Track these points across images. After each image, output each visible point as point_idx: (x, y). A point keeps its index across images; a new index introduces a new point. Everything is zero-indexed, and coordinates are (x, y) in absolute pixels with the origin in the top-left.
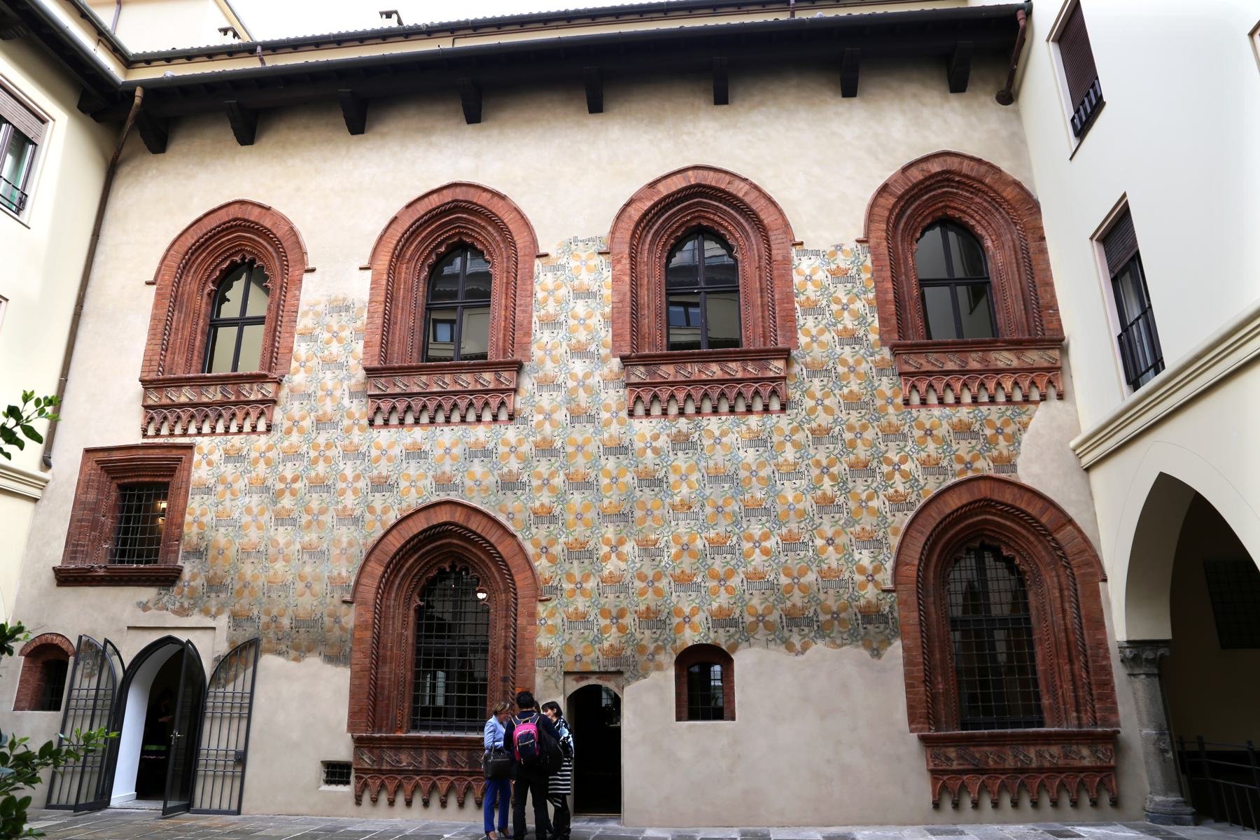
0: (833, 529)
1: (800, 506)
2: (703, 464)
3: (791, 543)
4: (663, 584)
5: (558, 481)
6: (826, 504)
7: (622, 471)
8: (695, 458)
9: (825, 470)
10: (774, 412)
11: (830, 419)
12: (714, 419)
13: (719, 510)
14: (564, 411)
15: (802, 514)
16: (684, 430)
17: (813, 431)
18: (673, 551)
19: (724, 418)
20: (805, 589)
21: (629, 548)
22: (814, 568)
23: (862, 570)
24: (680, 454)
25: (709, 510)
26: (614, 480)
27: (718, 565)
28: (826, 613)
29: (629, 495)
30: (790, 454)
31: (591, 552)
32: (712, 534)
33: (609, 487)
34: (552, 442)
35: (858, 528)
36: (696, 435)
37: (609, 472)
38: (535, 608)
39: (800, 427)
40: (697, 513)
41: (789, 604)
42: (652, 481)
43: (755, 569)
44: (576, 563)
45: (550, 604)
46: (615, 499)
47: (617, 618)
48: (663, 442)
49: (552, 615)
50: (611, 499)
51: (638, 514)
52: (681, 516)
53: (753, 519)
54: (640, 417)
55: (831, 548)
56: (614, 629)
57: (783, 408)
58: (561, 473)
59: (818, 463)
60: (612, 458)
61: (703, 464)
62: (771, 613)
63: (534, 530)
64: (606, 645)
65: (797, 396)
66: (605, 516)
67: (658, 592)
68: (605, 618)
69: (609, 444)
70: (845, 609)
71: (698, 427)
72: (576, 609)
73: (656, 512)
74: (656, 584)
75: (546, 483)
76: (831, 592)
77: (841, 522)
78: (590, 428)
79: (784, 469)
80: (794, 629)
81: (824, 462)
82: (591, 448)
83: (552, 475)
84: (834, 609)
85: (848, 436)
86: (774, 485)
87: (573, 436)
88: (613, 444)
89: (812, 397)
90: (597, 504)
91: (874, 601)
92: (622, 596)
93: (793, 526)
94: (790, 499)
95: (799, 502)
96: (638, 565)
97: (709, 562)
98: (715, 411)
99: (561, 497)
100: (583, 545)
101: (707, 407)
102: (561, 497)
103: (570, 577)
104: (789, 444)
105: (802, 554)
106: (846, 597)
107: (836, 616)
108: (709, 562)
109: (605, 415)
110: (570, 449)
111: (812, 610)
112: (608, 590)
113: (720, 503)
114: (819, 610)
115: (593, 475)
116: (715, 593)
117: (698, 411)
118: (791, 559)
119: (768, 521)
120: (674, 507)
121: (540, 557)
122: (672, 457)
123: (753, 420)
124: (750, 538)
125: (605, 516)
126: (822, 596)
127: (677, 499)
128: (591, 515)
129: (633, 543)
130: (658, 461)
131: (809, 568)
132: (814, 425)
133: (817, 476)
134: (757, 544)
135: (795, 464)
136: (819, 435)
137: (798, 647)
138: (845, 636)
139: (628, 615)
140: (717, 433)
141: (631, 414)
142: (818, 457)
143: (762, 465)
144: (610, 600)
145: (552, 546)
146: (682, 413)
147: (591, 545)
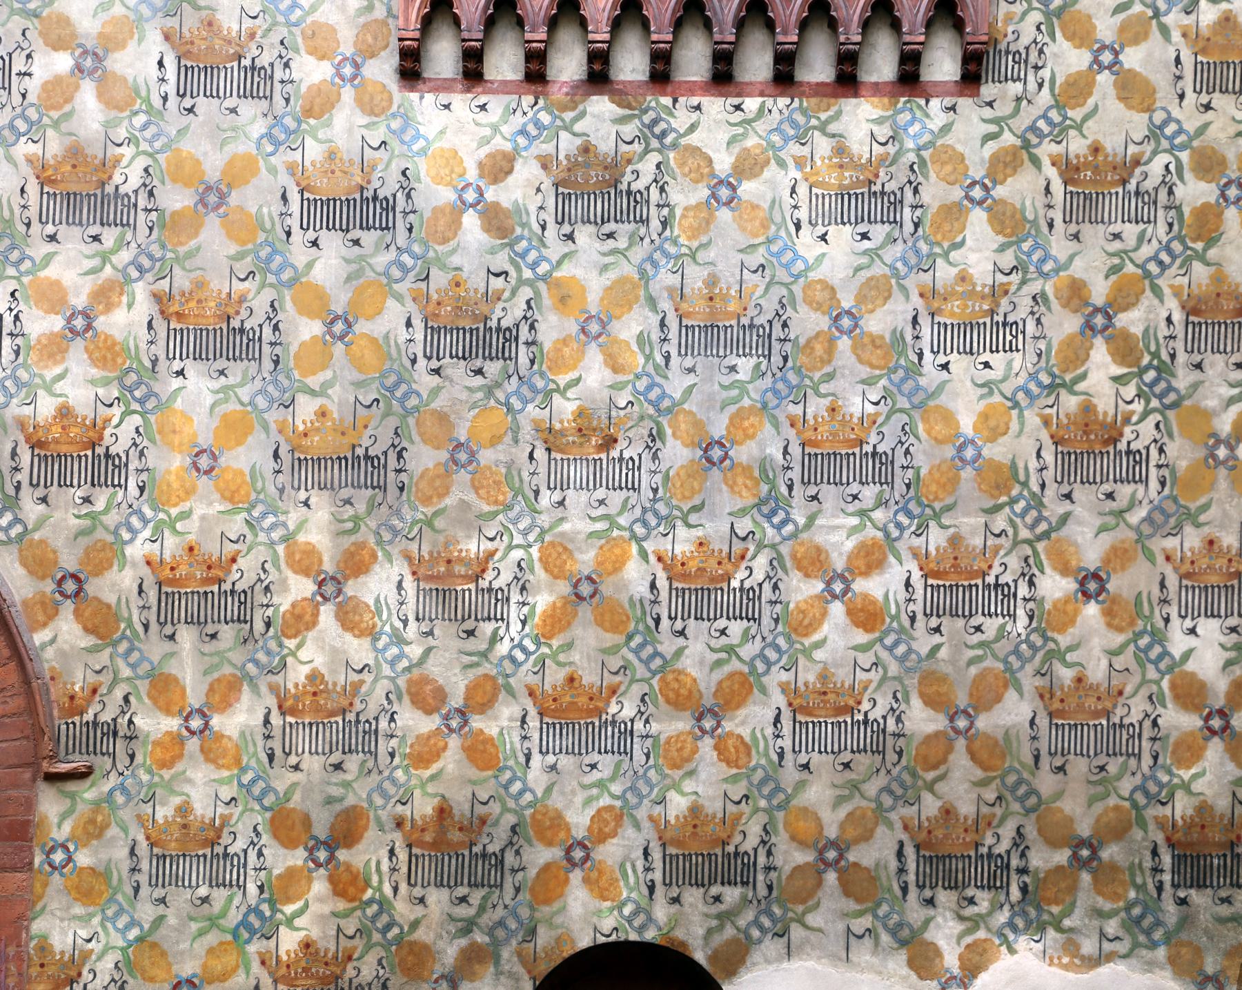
0: (1107, 539)
1: (997, 451)
2: (665, 278)
3: (956, 585)
4: (500, 722)
5: (128, 320)
6: (1089, 446)
7: (369, 292)
8: (638, 253)
9: (1099, 321)
10: (938, 90)
11: (1138, 124)
12: (715, 106)
13: (712, 454)
14: (154, 44)
15: (1002, 481)
16: (605, 145)
17: (1070, 170)
18: (542, 601)
19: (752, 104)
20: (988, 754)
21: (383, 584)
22: (1029, 681)
23: (1190, 693)
24: (584, 235)
25: (676, 453)
26: (340, 326)
27: (696, 656)
28: (1054, 843)
29: (392, 390)
30: (979, 253)
31: (244, 598)
32: (682, 543)
33: (319, 353)
34: (106, 166)
35: (1192, 539)
36: (647, 168)
37: (320, 295)
38: (30, 805)
39: (1022, 155)
40: (634, 465)
41: (931, 806)
42: (477, 336)
43: (824, 676)
44: (187, 636)
45: (88, 792)
46: (339, 399)
47: (331, 845)
48: (523, 189)
49: (93, 830)
50: (328, 397)
51: (424, 458)
52: (578, 472)
53: (829, 493)
54: (443, 86)
55: (1092, 610)
56: (319, 886)
57: (973, 73)
58: (141, 291)
59: (1076, 293)
60: (332, 242)
61: (665, 278)
62: (867, 836)
63: (31, 509)
64: (288, 941)
65: (1028, 32)
66: (303, 462)
67: (481, 752)
68: (289, 843)
69: (325, 187)
70: (1118, 831)
71: (654, 135)
72: (184, 810)
73: (487, 456)
74: (477, 722)
75: (81, 326)
76: (1078, 767)
77: (1135, 517)
78: (253, 119)
79: (953, 311)
80: (945, 897)
81: (1099, 291)
82: (257, 198)
83: (105, 296)
84: (1084, 829)
85: (1195, 192)
86: (915, 370)
87: (187, 146)
88: (340, 187)
89: (1081, 35)
90: (273, 416)
91: (1222, 804)
92: (352, 763)
93: (969, 523)
94: (967, 424)
95: (995, 434)
96: (415, 651)
97: (668, 645)
98: (723, 75)
99: (134, 381)
100: (217, 570)
101: (694, 59)
102: (134, 381)
103: (163, 689)
104: (978, 217)
105: (991, 626)
106: (1126, 786)
107: (1085, 854)
108: (668, 645)
109: (311, 71)
110: (175, 199)
111: (1008, 832)
112: (302, 739)
113: (718, 428)
114: (1031, 832)
115: (260, 304)
116: (679, 759)
117: (661, 72)
118: (950, 647)
119: (881, 503)
120: (551, 438)
121: (50, 612)
122: (555, 248)
123: (860, 119)
124: (813, 562)
125: (303, 462)
126: (1046, 782)
127: (565, 408)
128: (248, 457)
129: (399, 568)
130: (501, 261)
131: (1009, 679)
132: (1077, 146)
133: (1069, 342)
134: (837, 583)
135: (997, 292)
136: (1095, 185)
137: (951, 960)
138: (1112, 927)
139: (371, 833)
140: (723, 163)
141: (411, 69)
142: (1078, 269)
143: (876, 291)
144: (307, 778)
145: (100, 569)
146: (599, 75)
147: (246, 570)
